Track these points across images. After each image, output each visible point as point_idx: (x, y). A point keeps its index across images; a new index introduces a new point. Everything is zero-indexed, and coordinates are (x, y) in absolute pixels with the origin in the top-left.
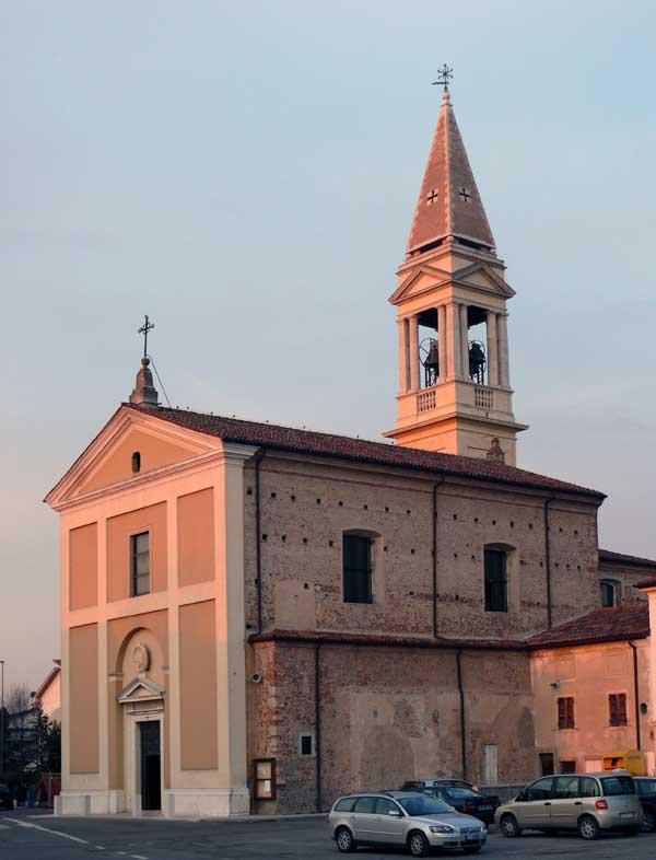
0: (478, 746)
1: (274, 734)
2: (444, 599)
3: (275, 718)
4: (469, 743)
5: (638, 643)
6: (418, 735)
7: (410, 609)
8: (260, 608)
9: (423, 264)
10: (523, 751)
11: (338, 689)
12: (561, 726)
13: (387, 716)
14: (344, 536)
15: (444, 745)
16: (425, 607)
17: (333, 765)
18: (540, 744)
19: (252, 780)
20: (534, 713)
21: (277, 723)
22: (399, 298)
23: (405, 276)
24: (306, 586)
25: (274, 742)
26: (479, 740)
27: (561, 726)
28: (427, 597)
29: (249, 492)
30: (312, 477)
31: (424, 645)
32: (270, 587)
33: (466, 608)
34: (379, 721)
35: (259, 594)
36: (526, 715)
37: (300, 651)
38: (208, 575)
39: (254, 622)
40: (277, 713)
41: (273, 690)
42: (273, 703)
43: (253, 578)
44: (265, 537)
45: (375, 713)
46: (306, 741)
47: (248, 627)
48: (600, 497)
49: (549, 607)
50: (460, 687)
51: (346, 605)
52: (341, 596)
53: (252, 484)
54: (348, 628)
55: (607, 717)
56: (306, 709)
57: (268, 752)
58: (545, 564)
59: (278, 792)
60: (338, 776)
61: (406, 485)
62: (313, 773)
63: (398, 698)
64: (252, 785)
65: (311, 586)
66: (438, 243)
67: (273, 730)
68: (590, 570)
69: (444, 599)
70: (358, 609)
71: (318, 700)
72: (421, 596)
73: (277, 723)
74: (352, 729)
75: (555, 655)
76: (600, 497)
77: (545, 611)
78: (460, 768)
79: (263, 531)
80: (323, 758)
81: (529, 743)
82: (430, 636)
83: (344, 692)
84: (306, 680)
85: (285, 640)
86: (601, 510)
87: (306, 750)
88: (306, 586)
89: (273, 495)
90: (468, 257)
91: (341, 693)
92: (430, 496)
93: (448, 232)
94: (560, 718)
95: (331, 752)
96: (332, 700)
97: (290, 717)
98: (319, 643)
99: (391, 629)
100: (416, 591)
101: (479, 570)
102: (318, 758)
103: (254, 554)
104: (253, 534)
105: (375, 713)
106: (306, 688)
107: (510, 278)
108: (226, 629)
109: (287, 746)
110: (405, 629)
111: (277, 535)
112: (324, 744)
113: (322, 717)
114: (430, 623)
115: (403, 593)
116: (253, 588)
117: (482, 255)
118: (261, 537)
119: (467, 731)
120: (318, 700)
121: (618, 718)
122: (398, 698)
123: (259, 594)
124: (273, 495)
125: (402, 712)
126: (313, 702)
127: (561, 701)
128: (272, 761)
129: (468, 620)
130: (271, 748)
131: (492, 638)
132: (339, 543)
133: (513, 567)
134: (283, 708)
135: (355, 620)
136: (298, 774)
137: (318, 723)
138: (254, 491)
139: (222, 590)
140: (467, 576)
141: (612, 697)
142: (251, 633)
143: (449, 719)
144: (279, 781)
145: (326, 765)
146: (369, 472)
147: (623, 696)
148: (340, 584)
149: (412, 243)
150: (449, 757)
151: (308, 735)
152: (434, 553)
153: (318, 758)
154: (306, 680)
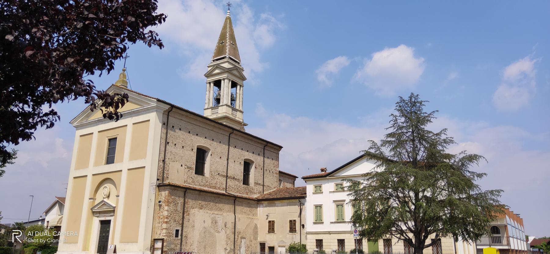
0: (239, 238)
1: (165, 227)
2: (230, 178)
3: (166, 220)
4: (236, 237)
5: (302, 200)
6: (219, 232)
7: (218, 180)
8: (163, 172)
9: (218, 64)
10: (254, 242)
12: (269, 232)
13: (209, 223)
14: (198, 149)
15: (228, 238)
16: (223, 180)
17: (186, 243)
18: (261, 239)
19: (152, 248)
20: (258, 226)
21: (166, 222)
22: (208, 75)
23: (210, 69)
24: (182, 165)
25: (164, 231)
26: (240, 236)
27: (269, 232)
28: (224, 176)
29: (164, 124)
30: (188, 122)
31: (223, 195)
33: (237, 183)
34: (206, 225)
35: (164, 167)
36: (256, 227)
37: (178, 192)
38: (144, 156)
39: (160, 178)
40: (167, 218)
41: (166, 208)
42: (166, 213)
43: (162, 159)
44: (168, 143)
45: (204, 221)
46: (177, 231)
47: (158, 180)
48: (281, 147)
49: (263, 185)
50: (235, 213)
51: (196, 176)
52: (194, 172)
53: (166, 121)
54: (196, 185)
55: (289, 229)
56: (178, 218)
57: (161, 236)
60: (188, 248)
61: (221, 132)
62: (179, 246)
63: (213, 216)
65: (183, 165)
66: (223, 58)
67: (165, 226)
68: (276, 173)
69: (230, 178)
70: (200, 177)
71: (183, 214)
72: (222, 175)
73: (166, 222)
74: (195, 227)
75: (268, 203)
76: (281, 147)
77: (262, 187)
78: (233, 247)
79: (168, 141)
80: (183, 240)
81: (256, 239)
82: (224, 192)
83: (194, 211)
84: (179, 205)
85: (174, 187)
86: (281, 152)
87: (177, 236)
88: (182, 165)
89: (173, 127)
91: (192, 211)
92: (228, 137)
94: (269, 229)
95: (186, 237)
96: (189, 214)
97: (172, 221)
98: (186, 191)
99: (211, 187)
100: (220, 173)
101: (242, 168)
102: (181, 239)
103: (164, 149)
104: (164, 141)
105: (204, 221)
106: (180, 208)
107: (245, 73)
108: (150, 177)
109: (170, 233)
110: (215, 188)
111: (173, 143)
112: (184, 234)
113: (185, 222)
114: (224, 186)
115: (216, 173)
116: (161, 164)
117: (237, 65)
118: (167, 143)
119: (236, 232)
120: (183, 214)
121: (292, 229)
122: (213, 216)
123: (164, 167)
124: (173, 127)
125: (214, 222)
126: (181, 214)
127: (270, 222)
128: (163, 240)
129: (236, 188)
130: (162, 234)
131: (245, 196)
132: (195, 150)
133: (252, 170)
134: (170, 216)
135: (197, 182)
136: (173, 246)
137: (183, 224)
138: (166, 124)
139: (150, 163)
140: (237, 170)
141: (291, 221)
142: (159, 182)
143: (230, 225)
144: (164, 250)
145: (184, 243)
146: (209, 124)
147: (295, 221)
148: (194, 167)
150: (229, 242)
151: (178, 229)
153: (181, 239)
154: (179, 205)
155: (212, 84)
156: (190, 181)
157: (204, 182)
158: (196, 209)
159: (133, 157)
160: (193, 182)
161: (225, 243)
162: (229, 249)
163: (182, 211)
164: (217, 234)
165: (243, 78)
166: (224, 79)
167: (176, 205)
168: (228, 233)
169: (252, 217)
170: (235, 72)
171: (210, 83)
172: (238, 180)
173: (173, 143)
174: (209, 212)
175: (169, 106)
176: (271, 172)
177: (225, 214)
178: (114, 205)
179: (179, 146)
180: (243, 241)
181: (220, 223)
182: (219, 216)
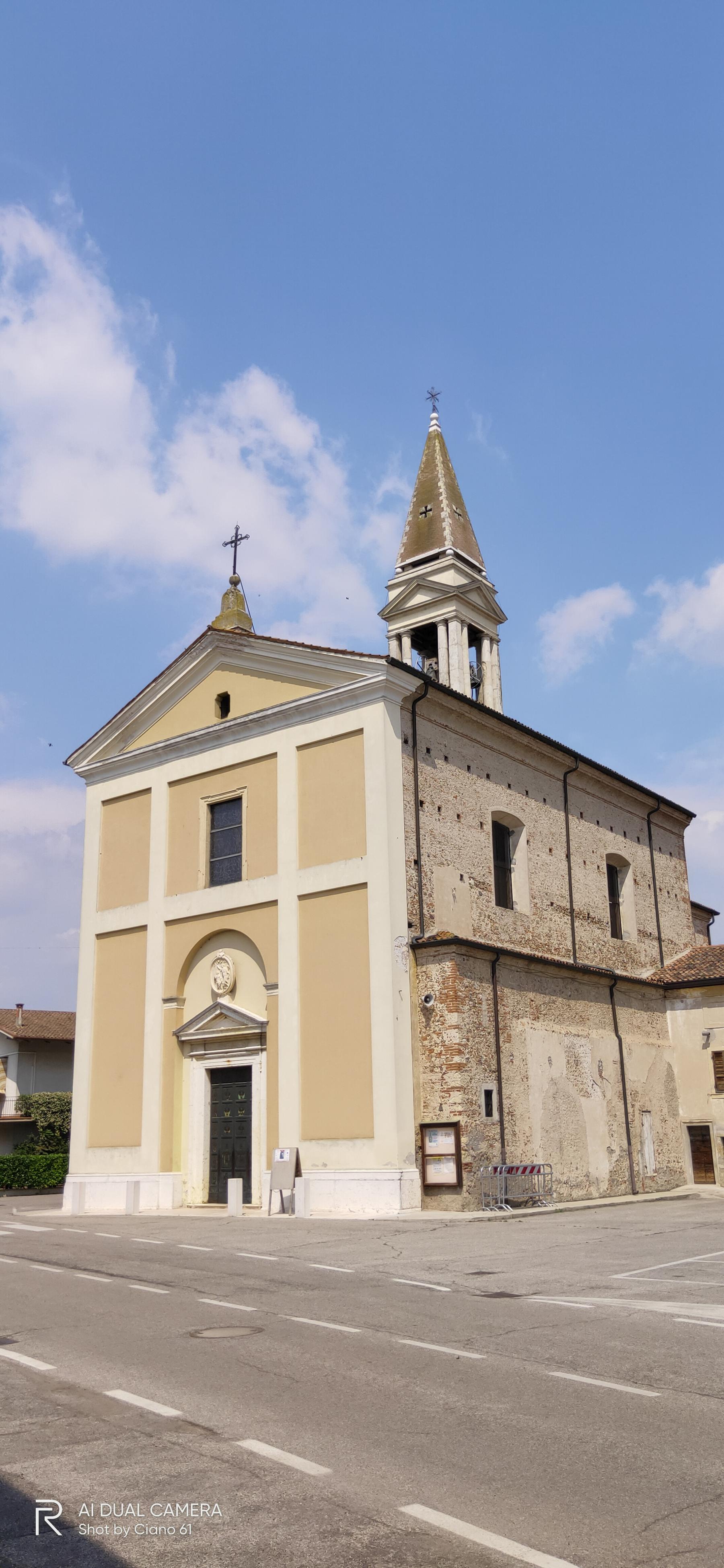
1: (458, 1084)
3: (457, 1059)
6: (587, 1095)
8: (421, 901)
11: (514, 1020)
16: (562, 922)
17: (514, 1134)
21: (459, 1067)
30: (464, 736)
32: (429, 873)
35: (420, 882)
38: (358, 849)
39: (416, 920)
40: (460, 1052)
41: (453, 1018)
44: (422, 803)
46: (488, 1094)
47: (410, 925)
49: (659, 939)
53: (410, 732)
54: (502, 941)
56: (487, 1052)
58: (652, 886)
59: (465, 1175)
61: (544, 766)
62: (498, 1145)
63: (567, 1041)
64: (420, 1162)
67: (455, 1078)
74: (531, 1082)
76: (690, 816)
77: (656, 944)
78: (625, 1146)
80: (506, 1125)
81: (674, 1114)
84: (484, 1007)
86: (688, 832)
90: (466, 575)
92: (560, 784)
93: (448, 546)
95: (511, 1113)
100: (555, 901)
102: (501, 1121)
104: (412, 798)
106: (486, 1018)
111: (433, 803)
118: (419, 804)
119: (628, 1092)
122: (567, 1041)
123: (420, 882)
124: (428, 750)
125: (572, 1060)
126: (492, 1040)
128: (455, 1126)
129: (594, 948)
132: (489, 827)
133: (627, 889)
134: (465, 1046)
136: (483, 1146)
137: (499, 1070)
140: (592, 890)
144: (466, 1159)
149: (403, 557)
150: (615, 1128)
152: (568, 856)
153: (501, 1121)
154: (484, 1007)
155: (407, 641)
156: (486, 927)
157: (521, 930)
158: (525, 1020)
159: (310, 857)
160: (495, 931)
161: (606, 1129)
162: (618, 1152)
163: (492, 1029)
164: (583, 1099)
165: (498, 618)
166: (446, 622)
167: (476, 1006)
168: (609, 1095)
169: (654, 1041)
170: (475, 598)
171: (399, 637)
172: (600, 921)
173: (433, 803)
174: (557, 1028)
175: (418, 682)
176: (673, 896)
177: (594, 1034)
178: (261, 1019)
179: (449, 813)
180: (647, 1119)
181: (588, 1065)
182: (583, 1041)
